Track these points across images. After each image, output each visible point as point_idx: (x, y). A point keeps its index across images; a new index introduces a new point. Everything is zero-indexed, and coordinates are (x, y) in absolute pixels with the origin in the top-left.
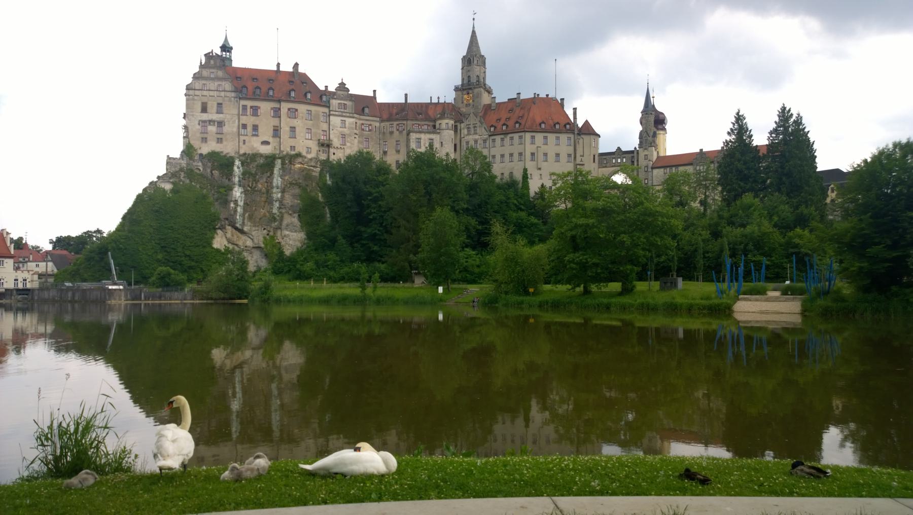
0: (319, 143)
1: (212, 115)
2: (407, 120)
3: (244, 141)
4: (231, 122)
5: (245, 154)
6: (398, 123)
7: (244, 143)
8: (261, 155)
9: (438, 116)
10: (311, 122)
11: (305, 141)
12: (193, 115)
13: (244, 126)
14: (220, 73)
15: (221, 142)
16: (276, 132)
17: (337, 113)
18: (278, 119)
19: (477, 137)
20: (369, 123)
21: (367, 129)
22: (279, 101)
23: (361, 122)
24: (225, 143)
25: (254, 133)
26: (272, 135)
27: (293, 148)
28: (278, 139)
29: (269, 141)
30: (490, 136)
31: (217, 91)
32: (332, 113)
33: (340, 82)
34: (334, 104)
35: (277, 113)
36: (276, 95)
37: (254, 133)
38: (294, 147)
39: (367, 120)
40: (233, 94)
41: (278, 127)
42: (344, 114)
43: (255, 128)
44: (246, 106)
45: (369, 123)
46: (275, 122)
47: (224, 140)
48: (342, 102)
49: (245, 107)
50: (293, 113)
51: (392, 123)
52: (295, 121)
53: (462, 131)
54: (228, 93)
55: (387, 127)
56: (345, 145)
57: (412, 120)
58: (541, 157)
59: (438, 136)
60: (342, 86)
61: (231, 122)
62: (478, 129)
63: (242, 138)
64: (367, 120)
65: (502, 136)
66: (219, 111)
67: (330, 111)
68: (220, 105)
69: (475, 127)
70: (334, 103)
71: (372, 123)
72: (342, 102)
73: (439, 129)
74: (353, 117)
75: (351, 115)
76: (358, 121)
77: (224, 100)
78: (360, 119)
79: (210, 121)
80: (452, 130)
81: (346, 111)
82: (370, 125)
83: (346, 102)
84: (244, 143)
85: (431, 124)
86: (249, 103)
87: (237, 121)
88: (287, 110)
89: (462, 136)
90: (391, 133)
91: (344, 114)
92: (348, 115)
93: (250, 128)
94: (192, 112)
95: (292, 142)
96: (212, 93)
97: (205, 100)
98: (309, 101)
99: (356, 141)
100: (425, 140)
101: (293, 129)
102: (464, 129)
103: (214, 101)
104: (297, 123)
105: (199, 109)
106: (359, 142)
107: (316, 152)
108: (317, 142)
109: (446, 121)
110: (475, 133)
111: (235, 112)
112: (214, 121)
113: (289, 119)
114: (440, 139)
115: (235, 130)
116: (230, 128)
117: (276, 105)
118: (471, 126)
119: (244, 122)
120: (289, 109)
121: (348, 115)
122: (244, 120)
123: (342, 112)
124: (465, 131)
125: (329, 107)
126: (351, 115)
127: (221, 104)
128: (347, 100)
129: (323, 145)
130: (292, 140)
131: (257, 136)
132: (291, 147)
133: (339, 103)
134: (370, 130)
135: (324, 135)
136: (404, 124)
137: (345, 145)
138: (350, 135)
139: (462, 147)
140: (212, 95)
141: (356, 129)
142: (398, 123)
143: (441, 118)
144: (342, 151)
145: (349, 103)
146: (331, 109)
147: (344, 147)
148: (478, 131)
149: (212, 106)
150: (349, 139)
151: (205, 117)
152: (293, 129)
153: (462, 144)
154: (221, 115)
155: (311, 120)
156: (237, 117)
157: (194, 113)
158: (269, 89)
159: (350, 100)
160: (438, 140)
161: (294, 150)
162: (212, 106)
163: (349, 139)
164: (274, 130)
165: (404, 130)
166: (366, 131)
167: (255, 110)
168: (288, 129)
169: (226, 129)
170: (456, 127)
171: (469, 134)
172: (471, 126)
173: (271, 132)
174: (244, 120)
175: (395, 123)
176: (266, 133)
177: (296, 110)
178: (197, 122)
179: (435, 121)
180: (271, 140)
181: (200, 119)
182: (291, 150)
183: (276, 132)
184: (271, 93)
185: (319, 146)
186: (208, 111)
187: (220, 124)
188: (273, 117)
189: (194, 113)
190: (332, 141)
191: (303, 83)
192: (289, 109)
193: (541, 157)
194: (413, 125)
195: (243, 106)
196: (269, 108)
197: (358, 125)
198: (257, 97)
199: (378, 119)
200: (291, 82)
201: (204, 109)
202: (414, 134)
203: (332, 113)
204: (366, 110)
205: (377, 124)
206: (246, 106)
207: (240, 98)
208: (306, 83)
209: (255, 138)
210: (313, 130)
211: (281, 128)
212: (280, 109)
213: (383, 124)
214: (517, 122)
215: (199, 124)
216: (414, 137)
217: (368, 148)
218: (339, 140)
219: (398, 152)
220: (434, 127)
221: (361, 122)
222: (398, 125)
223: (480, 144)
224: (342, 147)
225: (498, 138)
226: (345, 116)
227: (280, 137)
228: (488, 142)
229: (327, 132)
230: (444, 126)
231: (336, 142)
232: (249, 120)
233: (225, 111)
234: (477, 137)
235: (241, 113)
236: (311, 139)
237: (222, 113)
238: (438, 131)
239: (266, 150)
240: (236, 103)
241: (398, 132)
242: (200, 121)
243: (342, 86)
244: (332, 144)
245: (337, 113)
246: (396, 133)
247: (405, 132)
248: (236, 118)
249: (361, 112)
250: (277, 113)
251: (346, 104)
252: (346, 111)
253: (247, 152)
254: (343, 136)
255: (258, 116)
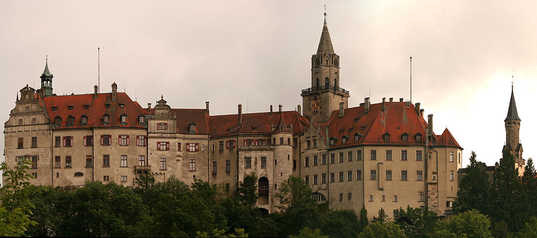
0: (135, 171)
1: (28, 151)
2: (237, 136)
3: (58, 174)
4: (44, 156)
5: (59, 187)
6: (228, 140)
7: (58, 176)
8: (74, 188)
9: (273, 129)
10: (127, 147)
11: (120, 169)
12: (11, 152)
13: (58, 159)
14: (34, 107)
15: (36, 177)
16: (90, 161)
17: (156, 135)
18: (91, 147)
19: (316, 152)
20: (195, 142)
21: (194, 150)
22: (92, 129)
23: (186, 141)
24: (39, 177)
25: (67, 165)
26: (85, 166)
27: (106, 178)
28: (91, 169)
29: (82, 172)
30: (329, 150)
31: (31, 125)
32: (150, 135)
33: (160, 99)
34: (153, 125)
35: (89, 141)
36: (90, 123)
37: (67, 165)
38: (108, 176)
39: (193, 139)
40: (46, 127)
41: (91, 156)
42: (164, 135)
43: (69, 159)
44: (60, 137)
45: (195, 142)
46: (87, 151)
47: (38, 174)
48: (162, 122)
49: (58, 139)
50: (106, 140)
51: (221, 140)
52: (108, 148)
53: (302, 145)
54: (42, 126)
55: (216, 145)
56: (166, 170)
57: (243, 136)
58: (383, 175)
59: (272, 153)
60: (162, 103)
61: (44, 156)
62: (318, 142)
63: (56, 171)
64: (193, 139)
65: (342, 151)
66: (34, 146)
67: (148, 133)
68: (34, 139)
69: (315, 140)
70: (153, 124)
71: (198, 142)
72: (162, 122)
73: (274, 145)
74: (175, 138)
75: (173, 135)
76: (181, 141)
77: (38, 134)
78: (184, 139)
79: (26, 156)
80: (289, 144)
81: (166, 131)
82: (197, 144)
83: (166, 122)
84: (58, 176)
85: (266, 138)
86: (62, 134)
87: (50, 154)
88: (100, 138)
89: (302, 151)
90: (221, 151)
91: (164, 135)
92: (169, 135)
93: (63, 161)
94: (10, 149)
95: (105, 171)
96: (27, 128)
97: (21, 135)
98: (124, 124)
99: (180, 164)
100: (256, 159)
101: (106, 158)
102: (303, 142)
103: (29, 136)
104: (113, 151)
105: (16, 145)
106: (183, 165)
107: (132, 181)
108: (133, 170)
109: (281, 135)
110: (315, 147)
111: (49, 144)
112: (29, 156)
113: (102, 147)
114: (274, 157)
115: (48, 163)
116: (44, 162)
117: (88, 133)
118: (311, 139)
119: (58, 155)
120: (102, 136)
121: (169, 135)
122: (57, 152)
123: (162, 133)
124: (305, 145)
125: (147, 129)
126: (173, 135)
127: (36, 138)
128: (167, 119)
129: (140, 172)
130: (105, 169)
131: (70, 167)
132: (105, 177)
133: (158, 124)
134: (196, 150)
135: (142, 161)
136: (234, 141)
137: (166, 170)
138: (172, 159)
139: (302, 164)
140: (28, 130)
141: (179, 150)
142: (228, 140)
143: (275, 132)
144: (163, 176)
145: (170, 122)
146: (149, 131)
147: (165, 172)
148: (318, 145)
149: (28, 142)
150: (170, 163)
151: (22, 152)
152: (106, 158)
153: (302, 161)
154: (35, 149)
155: (127, 145)
156: (50, 150)
157: (11, 150)
158: (82, 117)
159: (171, 119)
160: (272, 157)
161: (108, 180)
162: (28, 142)
163: (170, 163)
164: (87, 160)
165: (234, 147)
166: (192, 152)
167: (68, 140)
168: (101, 158)
169: (40, 163)
170: (295, 140)
171: (309, 148)
172: (311, 139)
173: (84, 163)
174: (57, 152)
175: (225, 140)
176: (79, 165)
177: (110, 136)
178: (14, 159)
179: (270, 135)
180: (83, 171)
181: (17, 155)
182: (105, 180)
183: (90, 161)
184: (84, 121)
185: (135, 173)
186: (23, 147)
187: (35, 158)
188: (85, 146)
189: (11, 150)
190: (150, 166)
191: (120, 105)
192: (102, 136)
193: (383, 175)
194: (245, 141)
195: (56, 137)
196: (82, 137)
197: (182, 146)
198: (70, 127)
199: (207, 136)
200: (107, 106)
201: (20, 146)
202: (243, 153)
203: (150, 135)
204: (193, 128)
205: (206, 143)
206: (60, 137)
207: (53, 130)
208: (124, 105)
209: (68, 170)
210: (128, 156)
211: (93, 158)
212: (92, 137)
213: (212, 142)
214: (356, 134)
215: (16, 161)
216: (243, 157)
217: (195, 171)
218: (158, 165)
219: (228, 172)
220: (269, 141)
221: (186, 141)
222: (227, 142)
223: (319, 161)
224: (162, 172)
225: (337, 153)
226: (165, 138)
227: (93, 167)
228: (327, 157)
229: (145, 158)
230: (278, 142)
231: (155, 167)
232: (62, 152)
233: (38, 145)
234: (316, 152)
235: (54, 146)
236: (127, 167)
237: (37, 148)
238: (272, 147)
239: (79, 182)
240: (49, 136)
241: (228, 150)
242: (16, 157)
243: (162, 103)
244: (150, 170)
245: (156, 135)
246: (226, 151)
247: (235, 150)
248: (49, 150)
249: (186, 130)
250: (89, 141)
251: (166, 124)
252: (166, 131)
253: (61, 186)
254: (164, 160)
255: (71, 146)
